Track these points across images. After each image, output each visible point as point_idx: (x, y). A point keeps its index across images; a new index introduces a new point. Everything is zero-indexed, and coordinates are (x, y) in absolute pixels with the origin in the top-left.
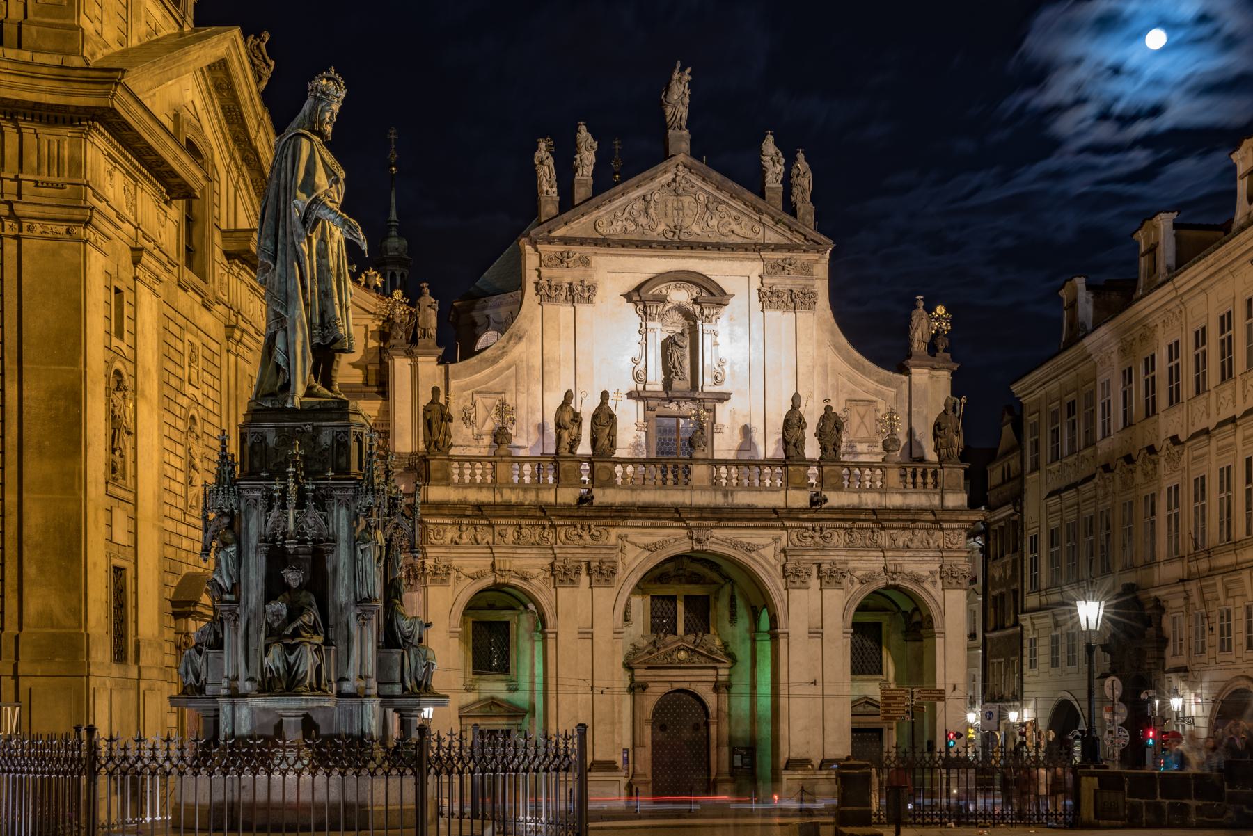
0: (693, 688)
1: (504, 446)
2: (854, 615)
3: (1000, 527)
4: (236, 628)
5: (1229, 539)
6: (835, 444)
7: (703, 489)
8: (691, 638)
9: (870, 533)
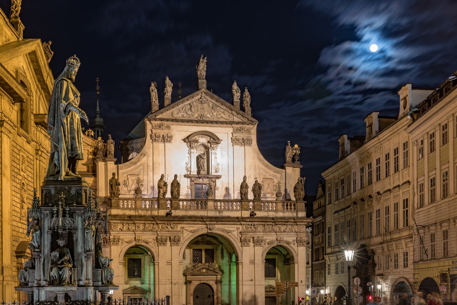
0: (208, 282)
1: (138, 195)
2: (266, 256)
3: (317, 224)
4: (40, 261)
5: (397, 228)
6: (259, 194)
7: (211, 210)
8: (207, 264)
9: (271, 226)
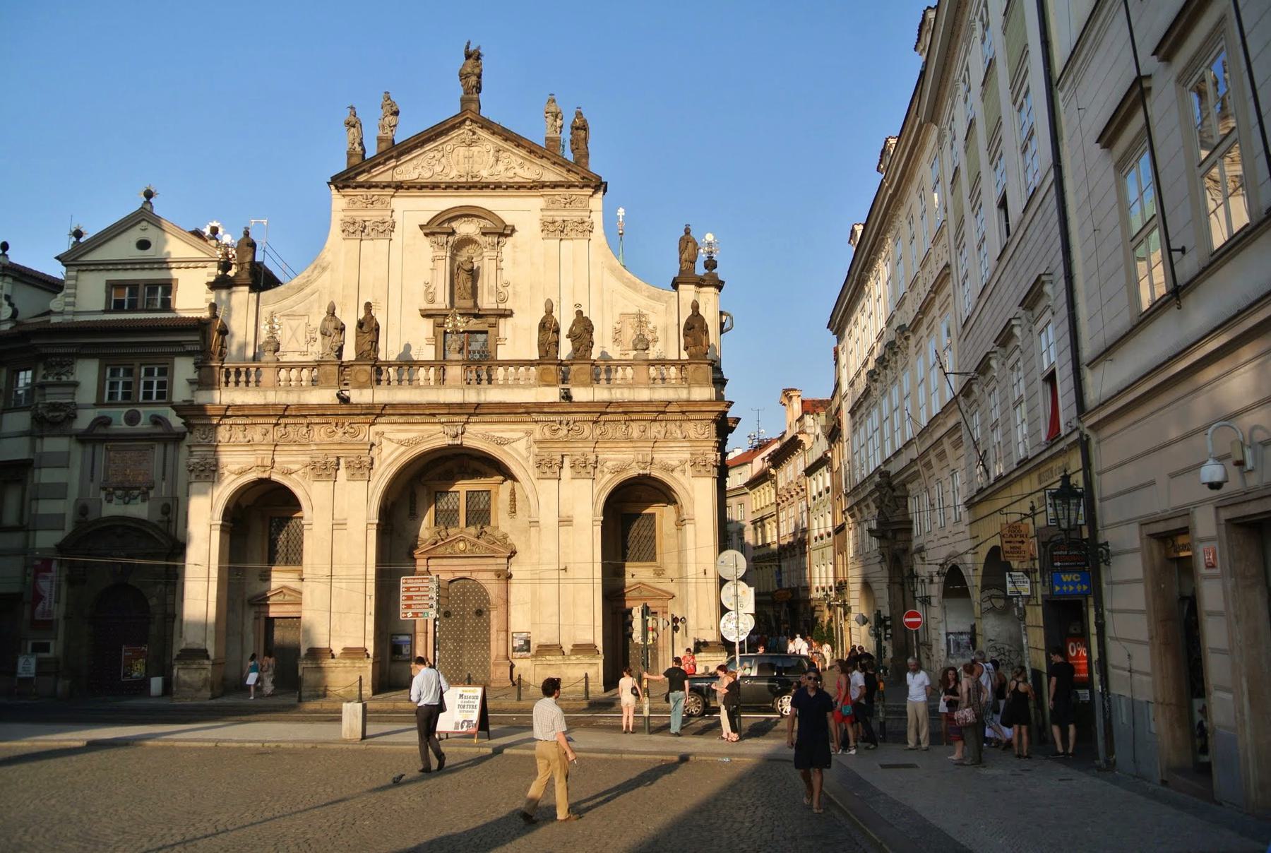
0: (474, 576)
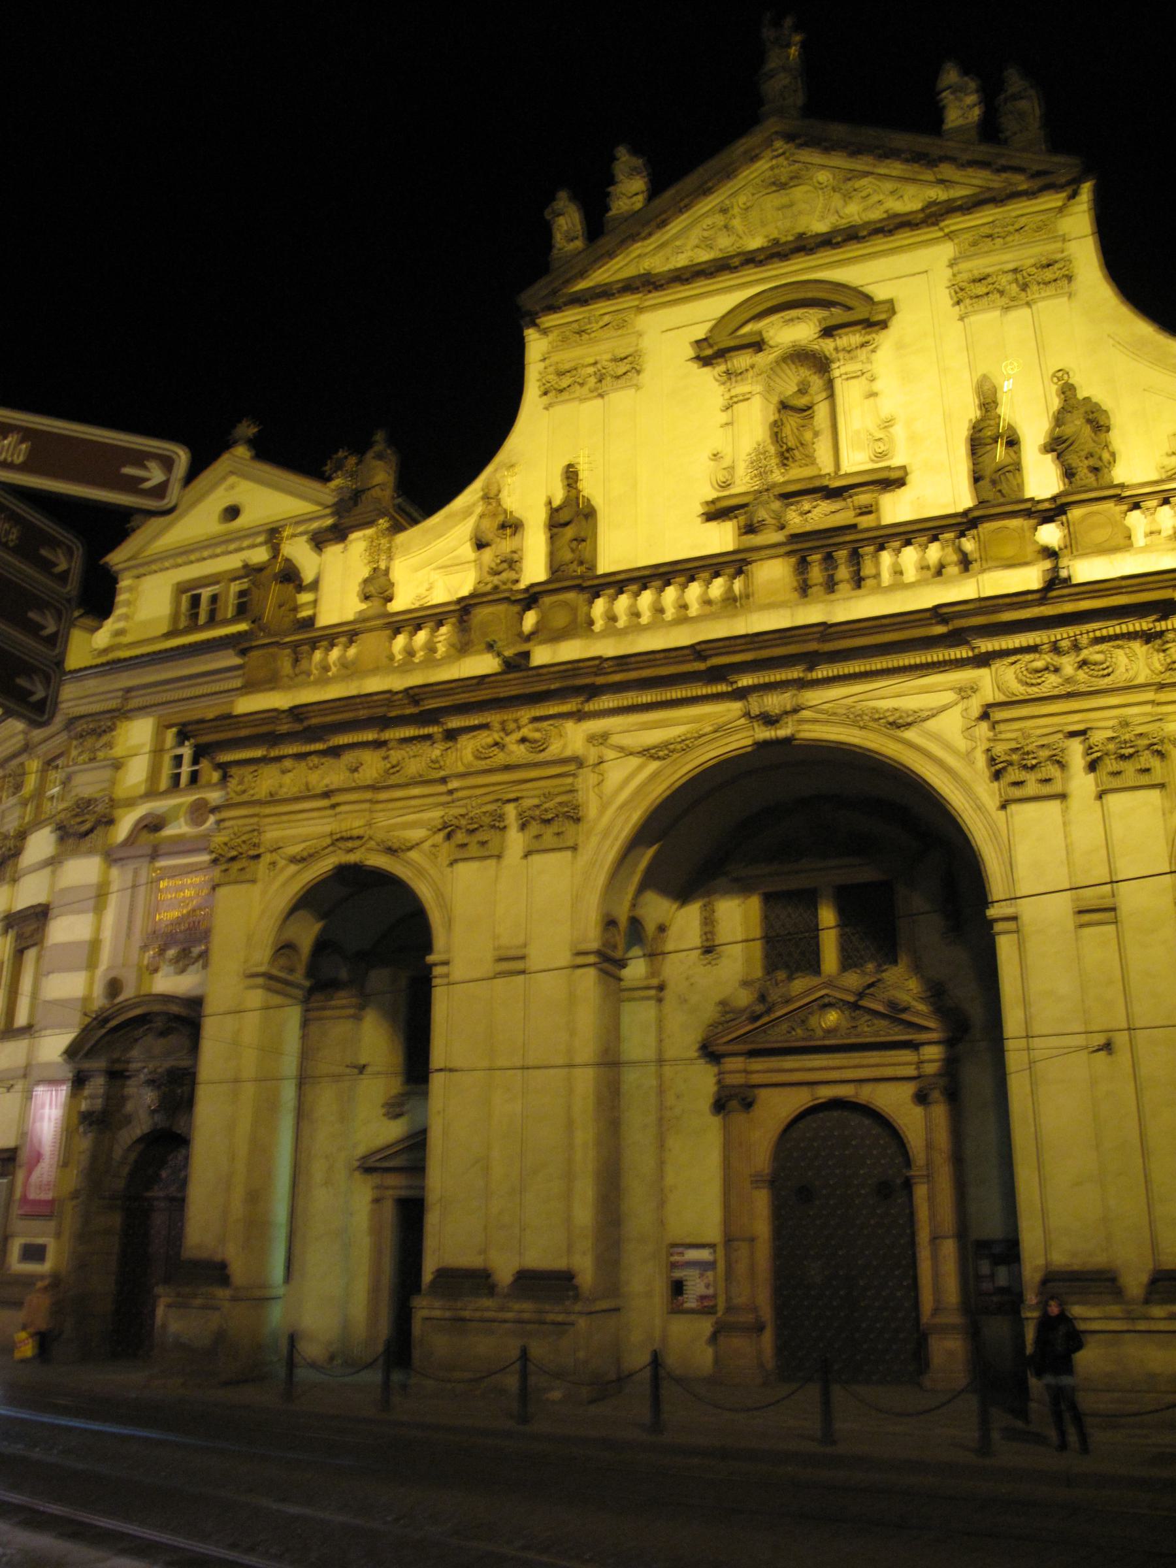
8: (853, 980)
